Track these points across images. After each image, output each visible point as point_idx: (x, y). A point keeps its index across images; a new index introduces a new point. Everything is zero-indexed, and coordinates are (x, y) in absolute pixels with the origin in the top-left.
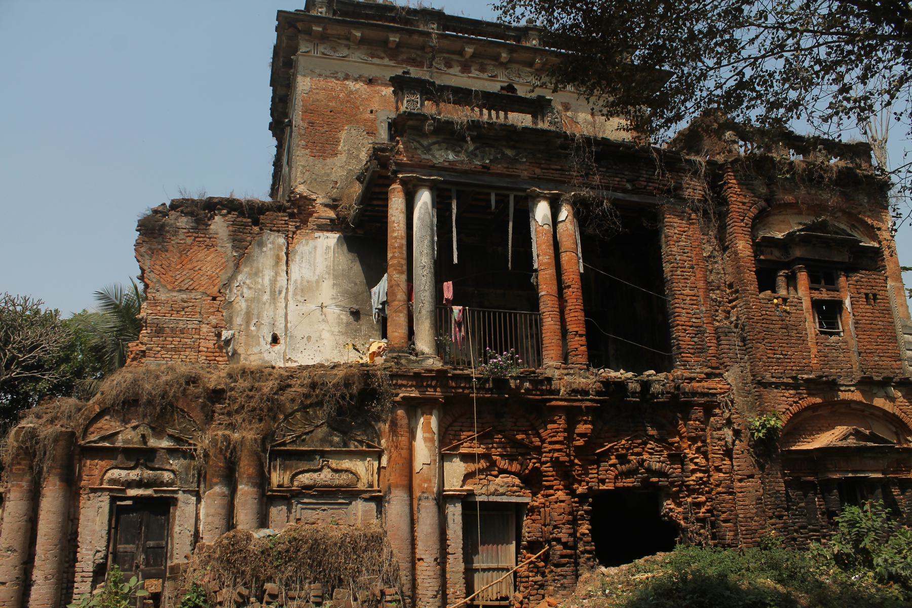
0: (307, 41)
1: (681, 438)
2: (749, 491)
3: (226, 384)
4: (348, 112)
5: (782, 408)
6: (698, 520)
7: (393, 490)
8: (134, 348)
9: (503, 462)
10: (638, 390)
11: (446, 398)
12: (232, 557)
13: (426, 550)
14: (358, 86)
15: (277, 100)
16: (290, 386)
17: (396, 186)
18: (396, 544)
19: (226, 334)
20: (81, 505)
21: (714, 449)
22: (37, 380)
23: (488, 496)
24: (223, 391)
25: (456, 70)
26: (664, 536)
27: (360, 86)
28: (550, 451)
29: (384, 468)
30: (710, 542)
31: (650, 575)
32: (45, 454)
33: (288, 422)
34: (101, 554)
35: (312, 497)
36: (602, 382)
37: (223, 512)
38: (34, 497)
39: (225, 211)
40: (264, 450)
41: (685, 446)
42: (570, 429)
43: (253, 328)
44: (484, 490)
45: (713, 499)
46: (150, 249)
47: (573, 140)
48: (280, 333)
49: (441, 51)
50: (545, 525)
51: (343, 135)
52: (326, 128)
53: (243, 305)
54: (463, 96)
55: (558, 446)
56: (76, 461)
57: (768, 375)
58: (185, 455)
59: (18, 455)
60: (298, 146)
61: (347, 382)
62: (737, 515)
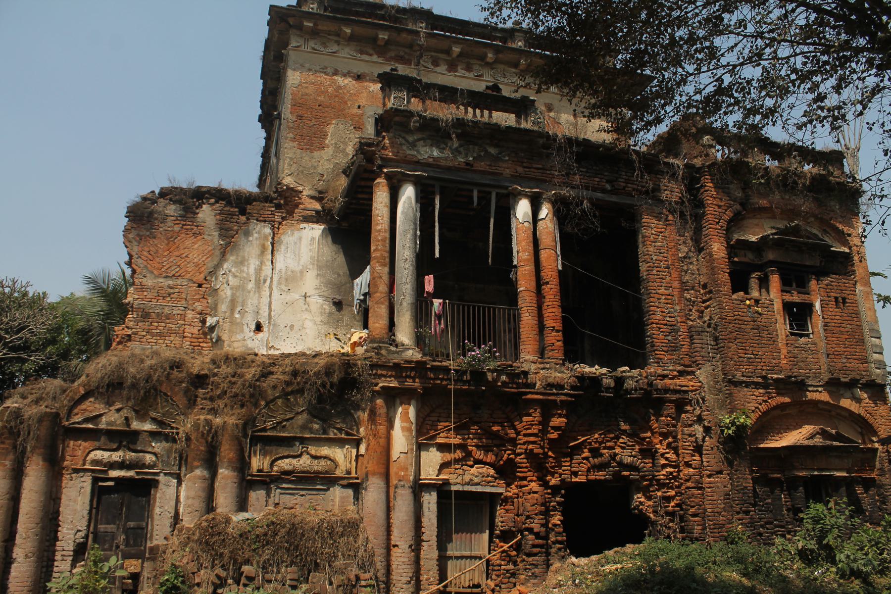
0: (298, 36)
1: (653, 433)
2: (718, 487)
3: (209, 370)
4: (336, 106)
5: (752, 406)
6: (668, 513)
7: (370, 478)
8: (120, 332)
9: (478, 453)
10: (612, 385)
11: (424, 389)
12: (211, 539)
13: (401, 537)
14: (346, 81)
15: (267, 93)
16: (272, 373)
17: (381, 180)
18: (372, 530)
19: (210, 321)
20: (64, 485)
21: (686, 445)
22: (24, 361)
23: (463, 485)
24: (206, 376)
25: (443, 68)
26: (634, 529)
27: (348, 81)
28: (524, 443)
29: (362, 456)
30: (679, 536)
31: (619, 566)
32: (29, 433)
33: (269, 408)
34: (82, 534)
35: (290, 482)
36: (577, 377)
37: (203, 495)
39: (213, 200)
40: (245, 435)
41: (656, 441)
42: (544, 422)
43: (237, 316)
44: (459, 480)
45: (682, 494)
46: (138, 235)
47: (555, 140)
48: (263, 321)
49: (429, 49)
50: (518, 515)
51: (331, 129)
53: (229, 292)
54: (448, 94)
55: (532, 439)
56: (60, 442)
57: (739, 374)
61: (328, 371)
62: (705, 510)
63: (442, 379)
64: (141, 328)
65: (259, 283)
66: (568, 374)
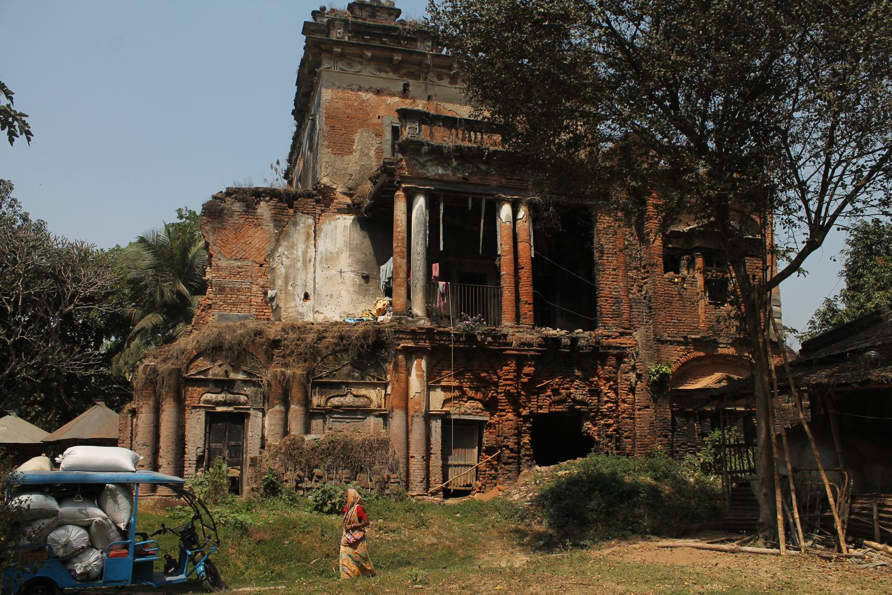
1: (599, 378)
2: (644, 416)
5: (674, 359)
6: (607, 436)
11: (432, 347)
12: (293, 452)
13: (417, 451)
14: (368, 96)
16: (325, 337)
18: (397, 446)
19: (270, 293)
20: (186, 417)
21: (623, 387)
22: (90, 310)
24: (279, 341)
25: (446, 82)
26: (583, 446)
27: (370, 96)
28: (504, 386)
30: (615, 452)
34: (201, 450)
37: (281, 423)
38: (157, 411)
40: (308, 382)
42: (518, 371)
43: (290, 288)
44: (457, 411)
45: (618, 422)
46: (213, 228)
51: (357, 137)
53: (283, 271)
54: (450, 123)
55: (509, 382)
57: (666, 335)
58: (257, 385)
60: (322, 145)
61: (365, 336)
62: (635, 434)
64: (219, 299)
65: (306, 262)
66: (536, 335)
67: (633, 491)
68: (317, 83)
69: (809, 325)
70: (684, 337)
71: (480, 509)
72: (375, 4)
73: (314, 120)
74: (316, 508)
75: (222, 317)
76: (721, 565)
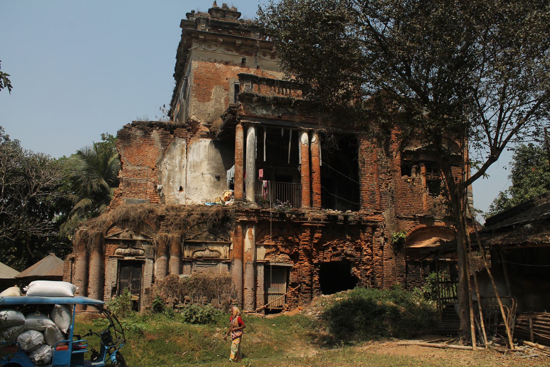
1: (361, 240)
2: (389, 264)
4: (215, 79)
5: (407, 229)
6: (366, 276)
11: (259, 221)
12: (172, 285)
13: (249, 285)
14: (220, 66)
16: (192, 214)
19: (159, 187)
21: (376, 246)
22: (46, 196)
24: (164, 216)
25: (268, 57)
26: (351, 282)
27: (221, 66)
28: (302, 245)
30: (371, 286)
37: (165, 267)
38: (88, 259)
39: (158, 128)
40: (182, 242)
42: (312, 236)
43: (171, 184)
44: (273, 261)
45: (373, 268)
46: (124, 146)
48: (183, 186)
50: (299, 276)
51: (213, 91)
52: (205, 87)
53: (167, 173)
54: (271, 83)
55: (306, 243)
57: (402, 214)
59: (81, 242)
61: (217, 213)
62: (383, 275)
63: (266, 217)
65: (181, 168)
66: (323, 214)
67: (382, 310)
68: (189, 57)
69: (490, 208)
70: (413, 216)
71: (287, 321)
72: (225, 9)
73: (187, 80)
74: (186, 320)
75: (129, 201)
76: (436, 356)
